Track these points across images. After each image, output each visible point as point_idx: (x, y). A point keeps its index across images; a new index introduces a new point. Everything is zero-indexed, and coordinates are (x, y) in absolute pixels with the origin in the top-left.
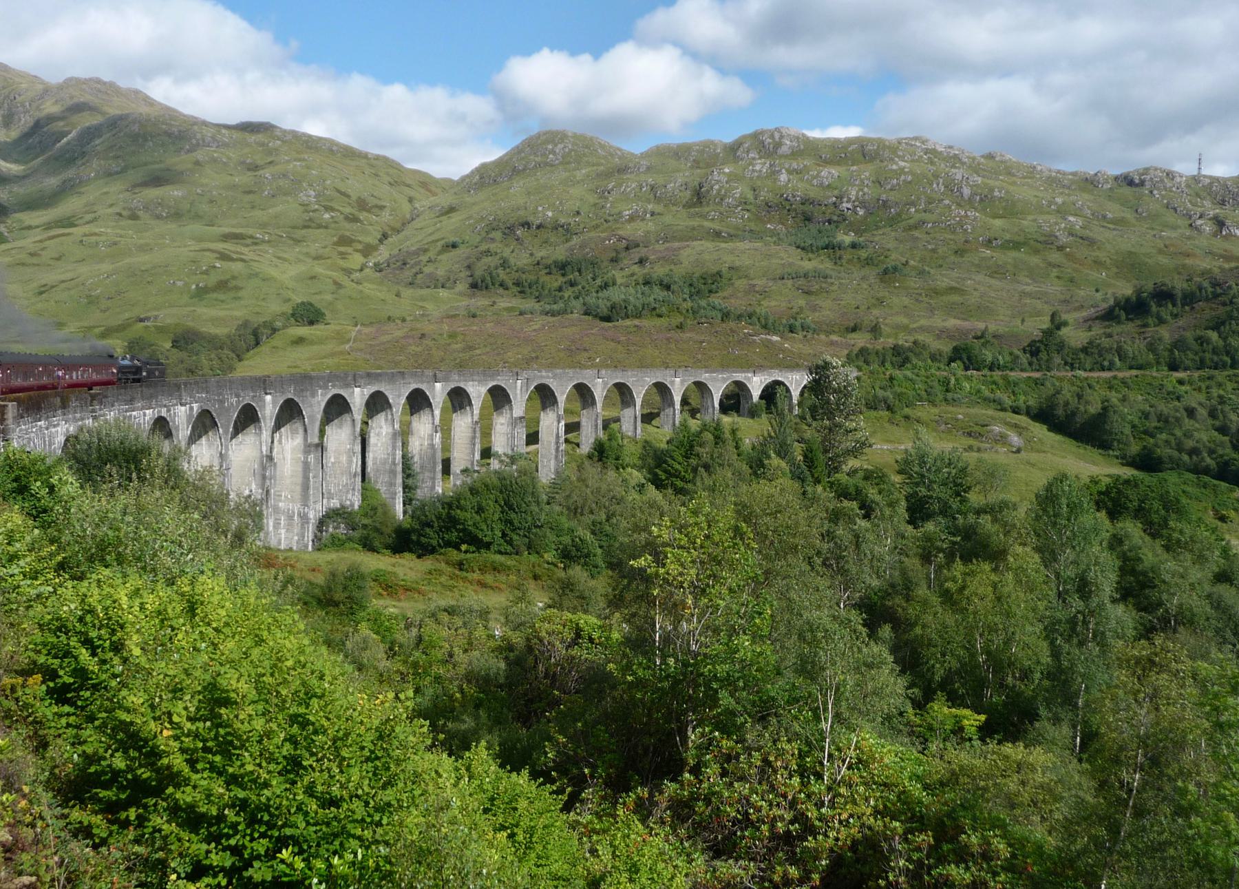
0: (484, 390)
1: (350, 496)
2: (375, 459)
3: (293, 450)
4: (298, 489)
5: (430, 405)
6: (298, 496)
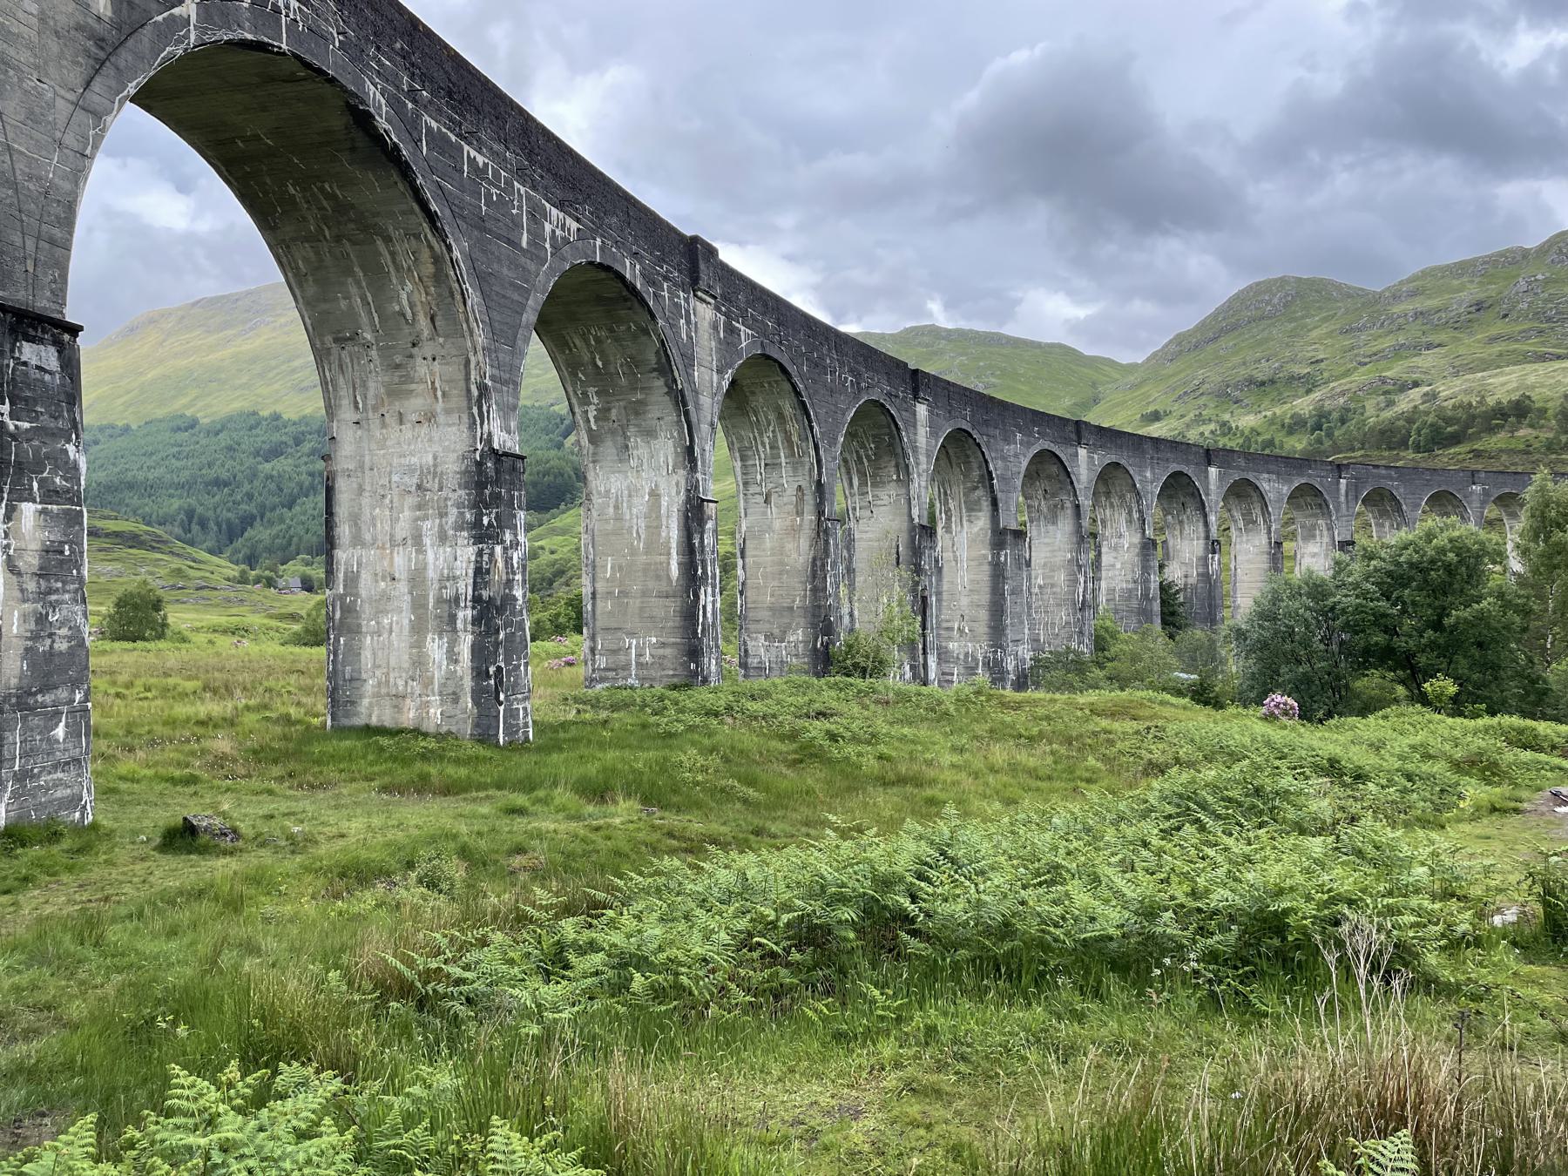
0: (1286, 490)
1: (1074, 645)
2: (1111, 591)
3: (972, 542)
4: (984, 615)
6: (982, 629)
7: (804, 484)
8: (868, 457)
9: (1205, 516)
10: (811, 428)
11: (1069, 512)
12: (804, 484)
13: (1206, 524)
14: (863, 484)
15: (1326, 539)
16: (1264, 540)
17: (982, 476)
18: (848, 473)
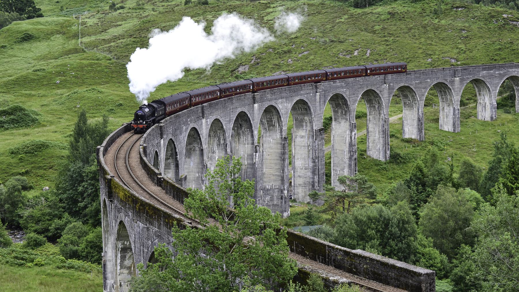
0: (290, 106)
5: (250, 127)
9: (252, 132)
11: (198, 152)
13: (252, 136)
15: (309, 128)
16: (278, 136)
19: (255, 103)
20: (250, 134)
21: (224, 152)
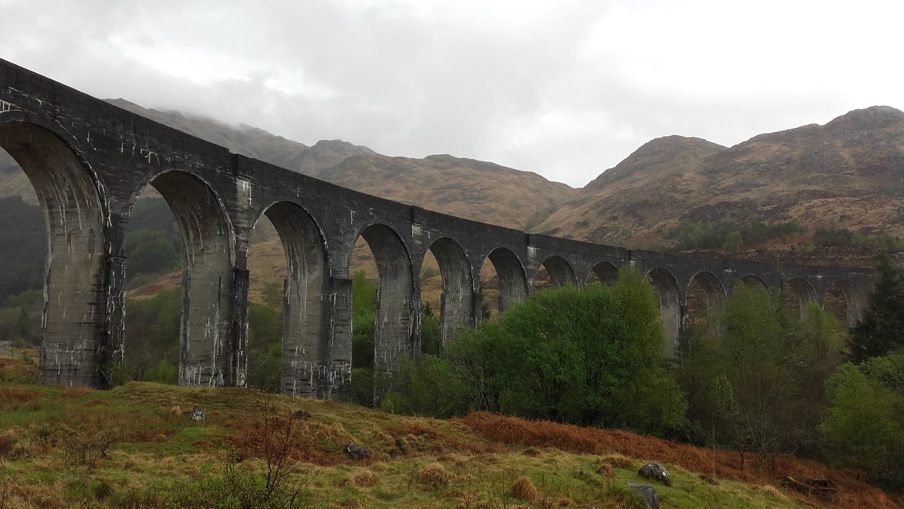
3: (310, 286)
4: (315, 340)
7: (95, 228)
8: (198, 216)
9: (525, 280)
10: (96, 185)
11: (406, 270)
12: (95, 228)
14: (197, 236)
17: (316, 239)
18: (186, 228)
19: (528, 244)
20: (523, 282)
21: (469, 291)
